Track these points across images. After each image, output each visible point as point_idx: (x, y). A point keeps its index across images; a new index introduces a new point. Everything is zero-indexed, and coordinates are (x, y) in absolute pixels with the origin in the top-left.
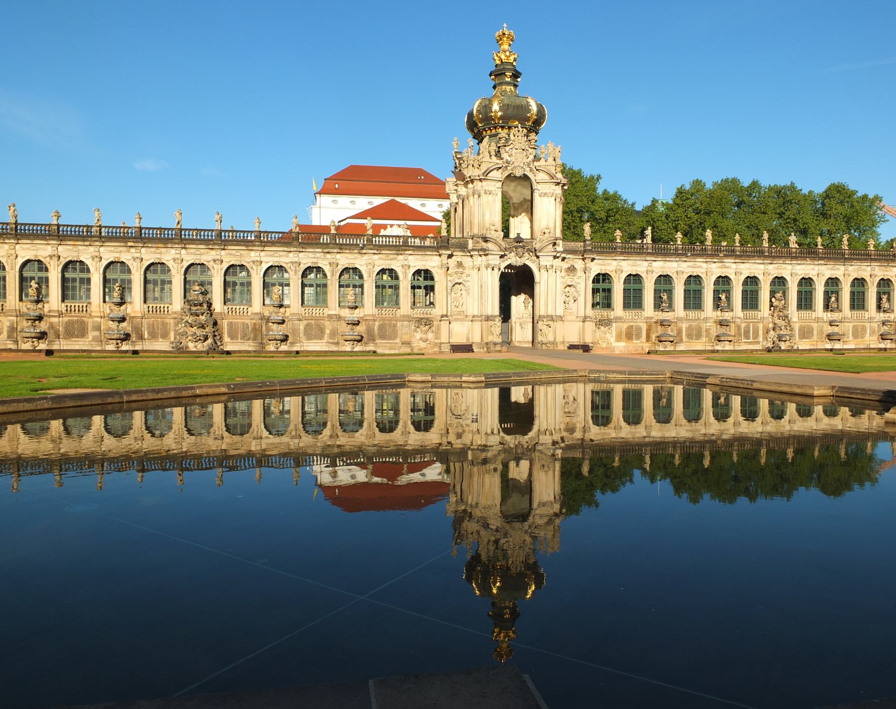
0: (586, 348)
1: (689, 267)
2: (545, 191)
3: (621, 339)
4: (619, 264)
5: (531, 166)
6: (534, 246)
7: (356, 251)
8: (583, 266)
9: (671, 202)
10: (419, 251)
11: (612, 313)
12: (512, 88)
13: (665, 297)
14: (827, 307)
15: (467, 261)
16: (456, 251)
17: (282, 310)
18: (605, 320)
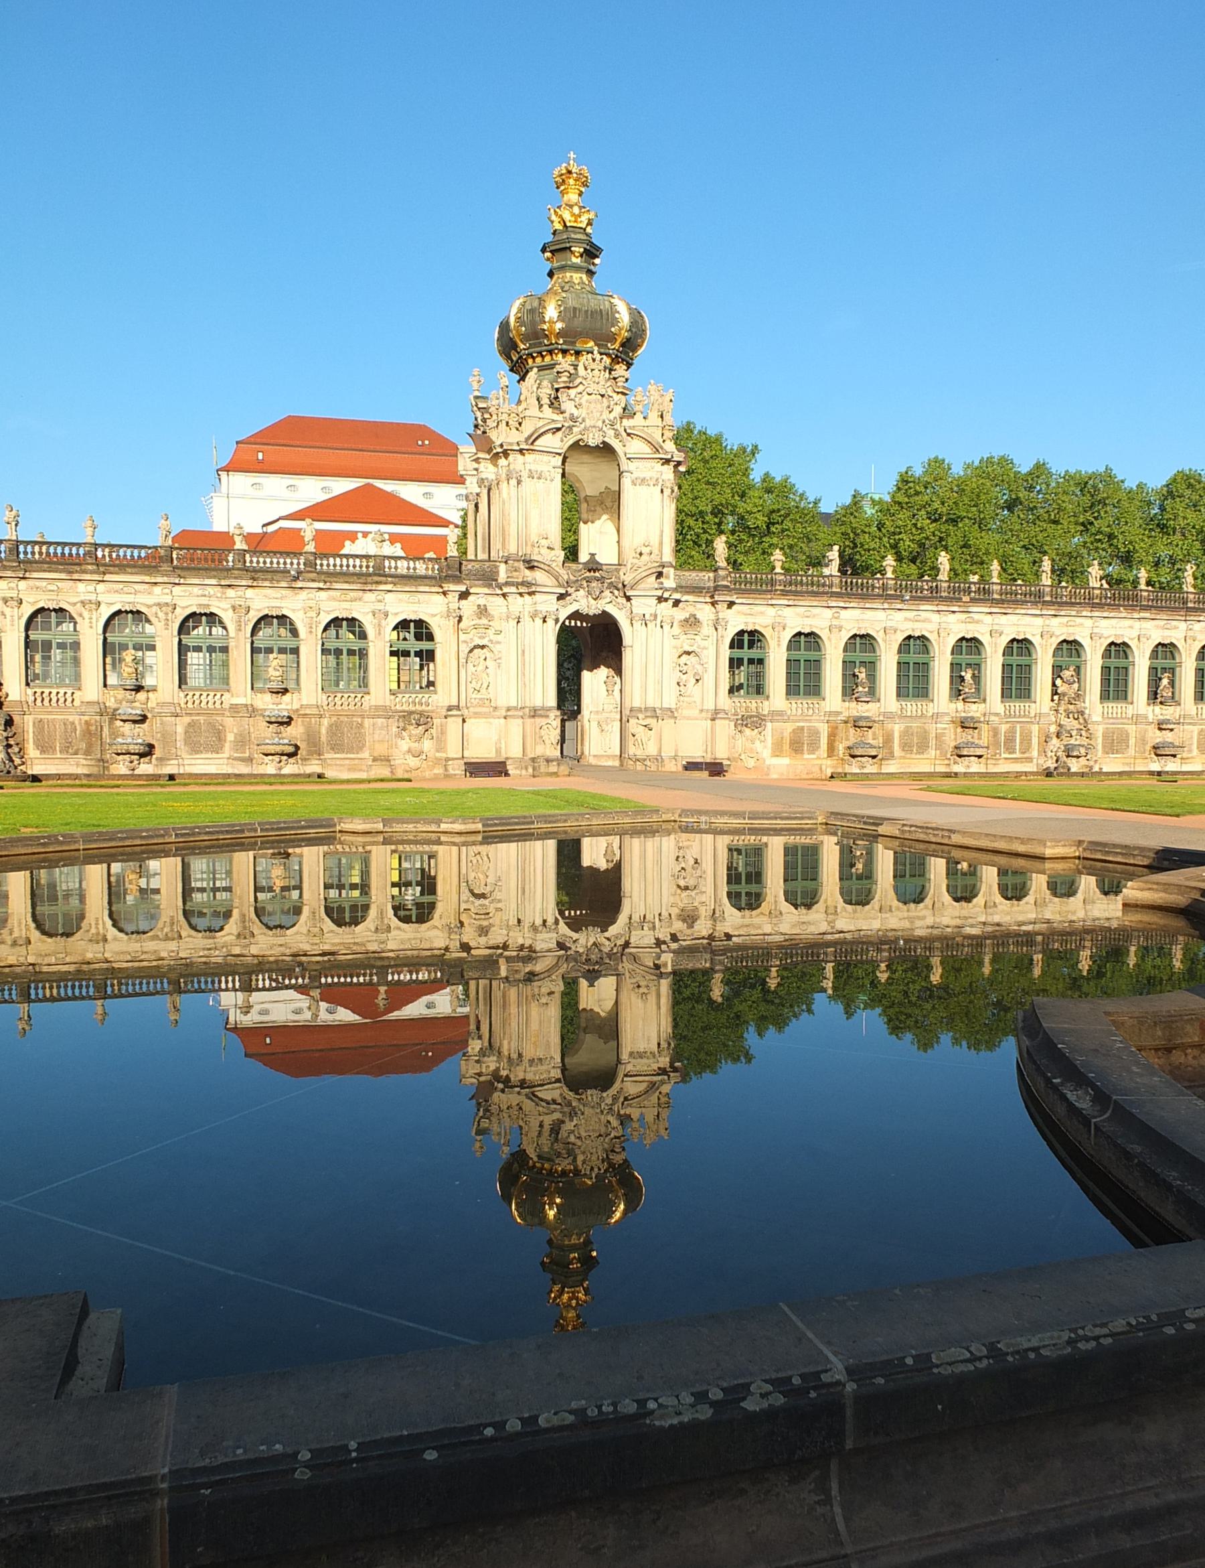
0: (716, 769)
1: (906, 619)
2: (642, 476)
3: (781, 751)
4: (779, 612)
5: (617, 426)
6: (622, 577)
7: (284, 584)
8: (713, 617)
9: (887, 498)
10: (406, 585)
11: (766, 703)
12: (584, 277)
13: (862, 676)
14: (1154, 695)
15: (496, 605)
16: (476, 586)
17: (141, 696)
18: (751, 717)
